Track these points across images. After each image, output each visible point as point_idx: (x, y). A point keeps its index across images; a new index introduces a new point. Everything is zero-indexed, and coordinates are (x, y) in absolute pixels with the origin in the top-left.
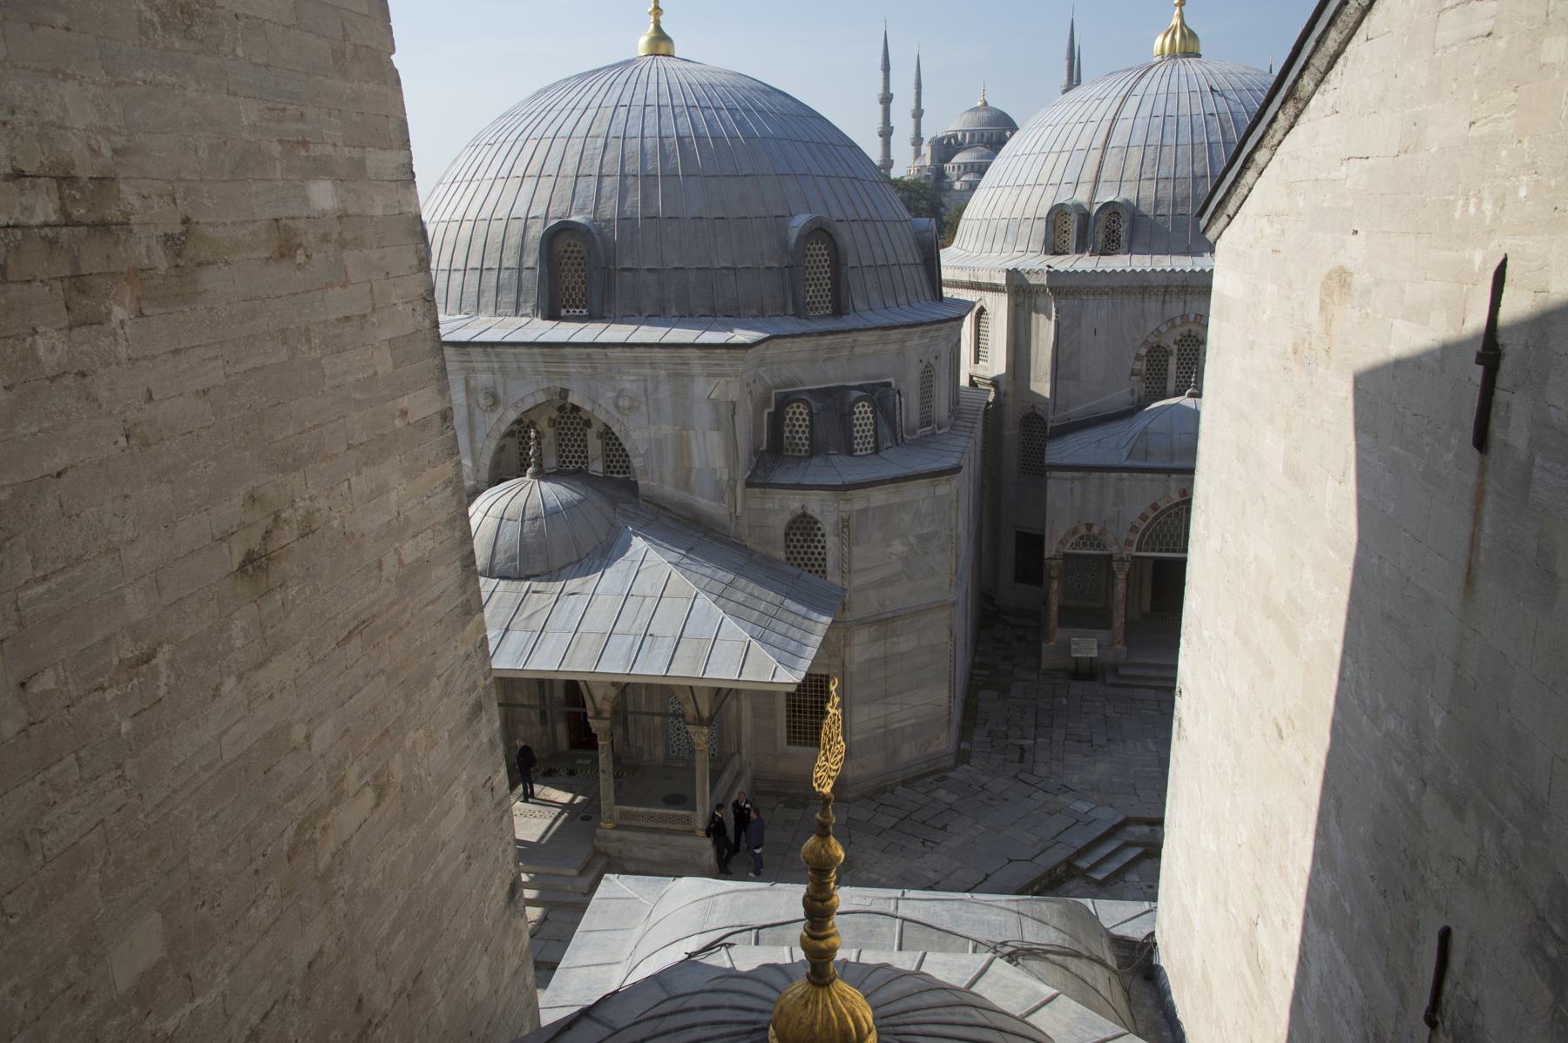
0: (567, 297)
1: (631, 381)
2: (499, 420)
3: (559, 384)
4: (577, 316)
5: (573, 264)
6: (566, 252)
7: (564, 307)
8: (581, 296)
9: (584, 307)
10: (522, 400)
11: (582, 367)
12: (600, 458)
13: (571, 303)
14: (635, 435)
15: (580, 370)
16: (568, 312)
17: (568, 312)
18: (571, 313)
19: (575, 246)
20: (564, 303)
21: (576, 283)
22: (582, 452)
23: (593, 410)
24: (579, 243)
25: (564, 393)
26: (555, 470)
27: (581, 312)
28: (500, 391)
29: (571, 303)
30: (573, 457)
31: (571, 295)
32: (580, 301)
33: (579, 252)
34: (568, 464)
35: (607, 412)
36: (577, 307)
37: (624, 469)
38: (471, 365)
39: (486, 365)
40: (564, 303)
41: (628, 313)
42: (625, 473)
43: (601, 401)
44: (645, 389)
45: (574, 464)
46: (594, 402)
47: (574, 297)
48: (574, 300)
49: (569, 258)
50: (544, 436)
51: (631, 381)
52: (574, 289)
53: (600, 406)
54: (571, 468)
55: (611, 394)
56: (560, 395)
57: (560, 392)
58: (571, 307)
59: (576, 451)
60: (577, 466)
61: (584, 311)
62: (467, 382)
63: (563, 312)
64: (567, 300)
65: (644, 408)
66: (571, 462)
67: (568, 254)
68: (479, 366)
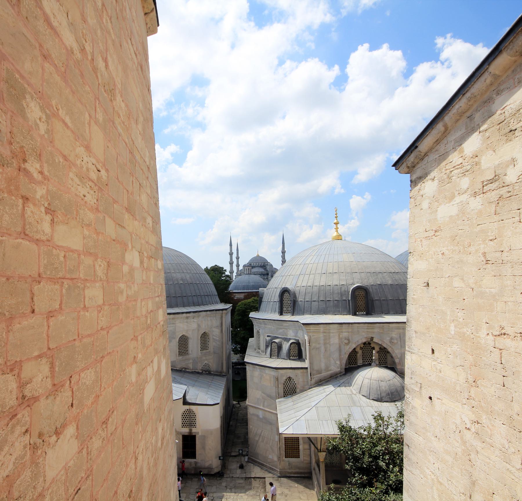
2: (349, 348)
3: (371, 336)
4: (362, 314)
5: (360, 298)
6: (358, 295)
7: (358, 312)
10: (358, 341)
11: (379, 330)
12: (378, 360)
14: (396, 351)
17: (359, 313)
19: (361, 293)
21: (362, 304)
24: (362, 292)
25: (372, 338)
28: (350, 338)
30: (367, 360)
31: (360, 308)
32: (363, 309)
33: (362, 295)
35: (387, 344)
36: (362, 312)
38: (342, 330)
39: (347, 330)
41: (379, 313)
42: (385, 364)
43: (385, 341)
44: (400, 337)
46: (382, 341)
48: (361, 309)
49: (359, 297)
50: (358, 353)
52: (361, 306)
53: (384, 342)
54: (366, 363)
55: (388, 338)
59: (368, 358)
62: (339, 336)
63: (357, 313)
64: (359, 309)
65: (399, 342)
66: (366, 361)
67: (359, 295)
68: (344, 330)
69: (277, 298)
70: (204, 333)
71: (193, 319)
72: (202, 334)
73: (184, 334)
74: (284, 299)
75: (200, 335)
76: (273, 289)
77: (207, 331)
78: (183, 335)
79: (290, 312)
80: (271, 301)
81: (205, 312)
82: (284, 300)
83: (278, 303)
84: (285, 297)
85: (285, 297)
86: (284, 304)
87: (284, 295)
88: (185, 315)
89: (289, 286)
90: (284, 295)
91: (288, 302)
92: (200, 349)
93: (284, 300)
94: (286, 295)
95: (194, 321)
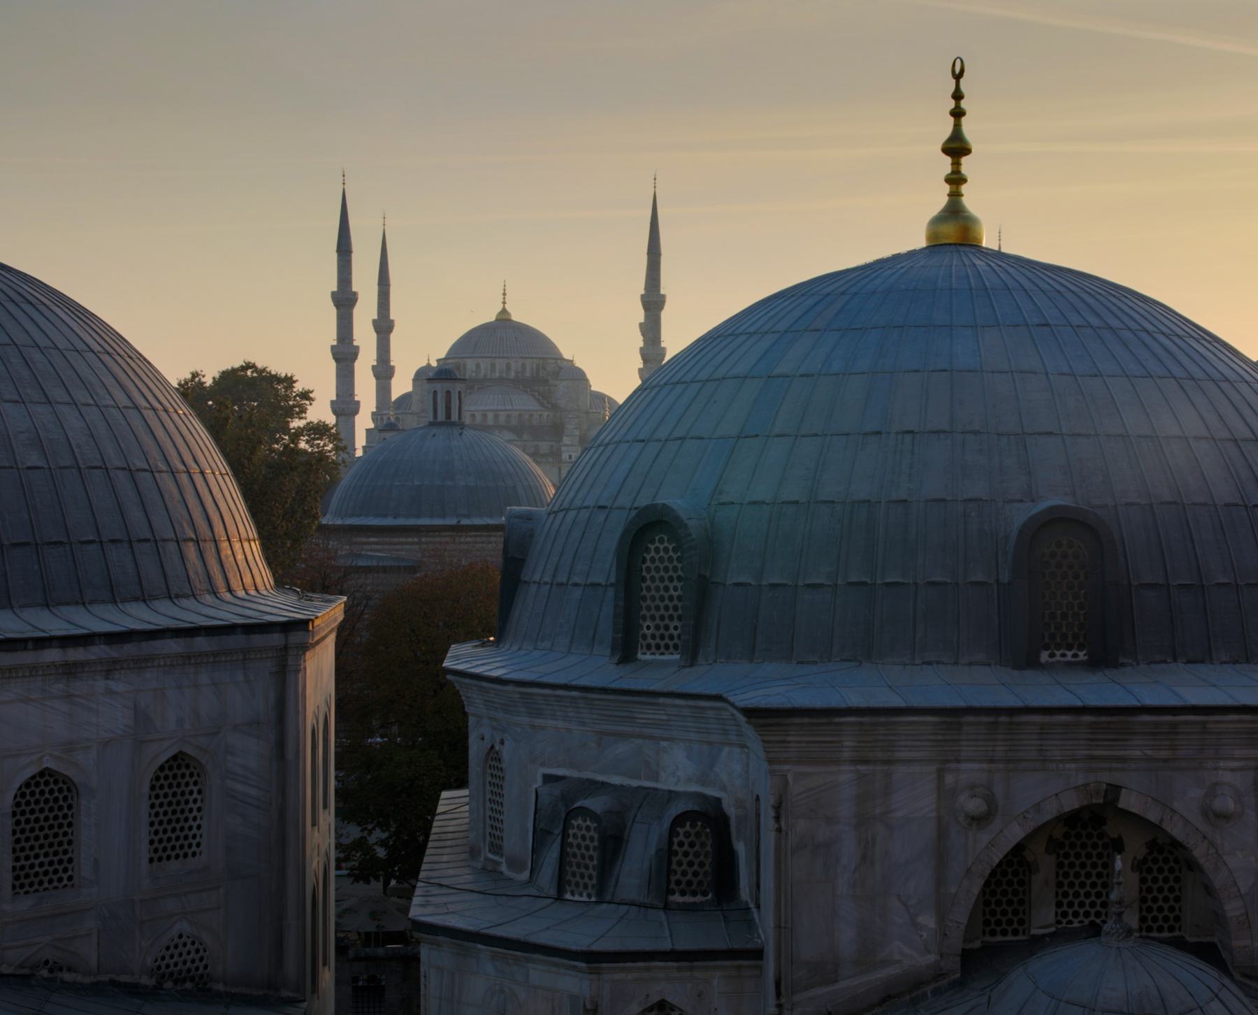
0: (1053, 630)
1: (1232, 770)
3: (1106, 778)
4: (1069, 664)
7: (1047, 647)
8: (1076, 629)
9: (1081, 647)
13: (1058, 640)
15: (1149, 752)
16: (1052, 655)
18: (1058, 658)
20: (1047, 640)
22: (1065, 895)
23: (1161, 820)
25: (1115, 790)
26: (1052, 929)
27: (1075, 656)
29: (1058, 640)
30: (1082, 905)
34: (1070, 917)
36: (1070, 648)
37: (1171, 922)
40: (1047, 640)
42: (1171, 929)
45: (1081, 918)
47: (1064, 630)
51: (1232, 770)
54: (1076, 925)
56: (1105, 797)
57: (1106, 791)
58: (1058, 647)
60: (1087, 921)
61: (1081, 654)
63: (1044, 657)
66: (1076, 914)
69: (605, 569)
70: (175, 758)
71: (107, 678)
72: (162, 768)
73: (49, 763)
74: (648, 570)
75: (150, 775)
76: (584, 514)
77: (188, 750)
78: (42, 774)
79: (676, 647)
80: (576, 579)
81: (181, 641)
82: (644, 579)
83: (611, 593)
84: (653, 560)
85: (653, 560)
86: (644, 599)
87: (648, 550)
88: (53, 655)
89: (675, 500)
90: (648, 550)
91: (667, 589)
92: (144, 850)
93: (644, 579)
94: (657, 550)
95: (110, 692)
